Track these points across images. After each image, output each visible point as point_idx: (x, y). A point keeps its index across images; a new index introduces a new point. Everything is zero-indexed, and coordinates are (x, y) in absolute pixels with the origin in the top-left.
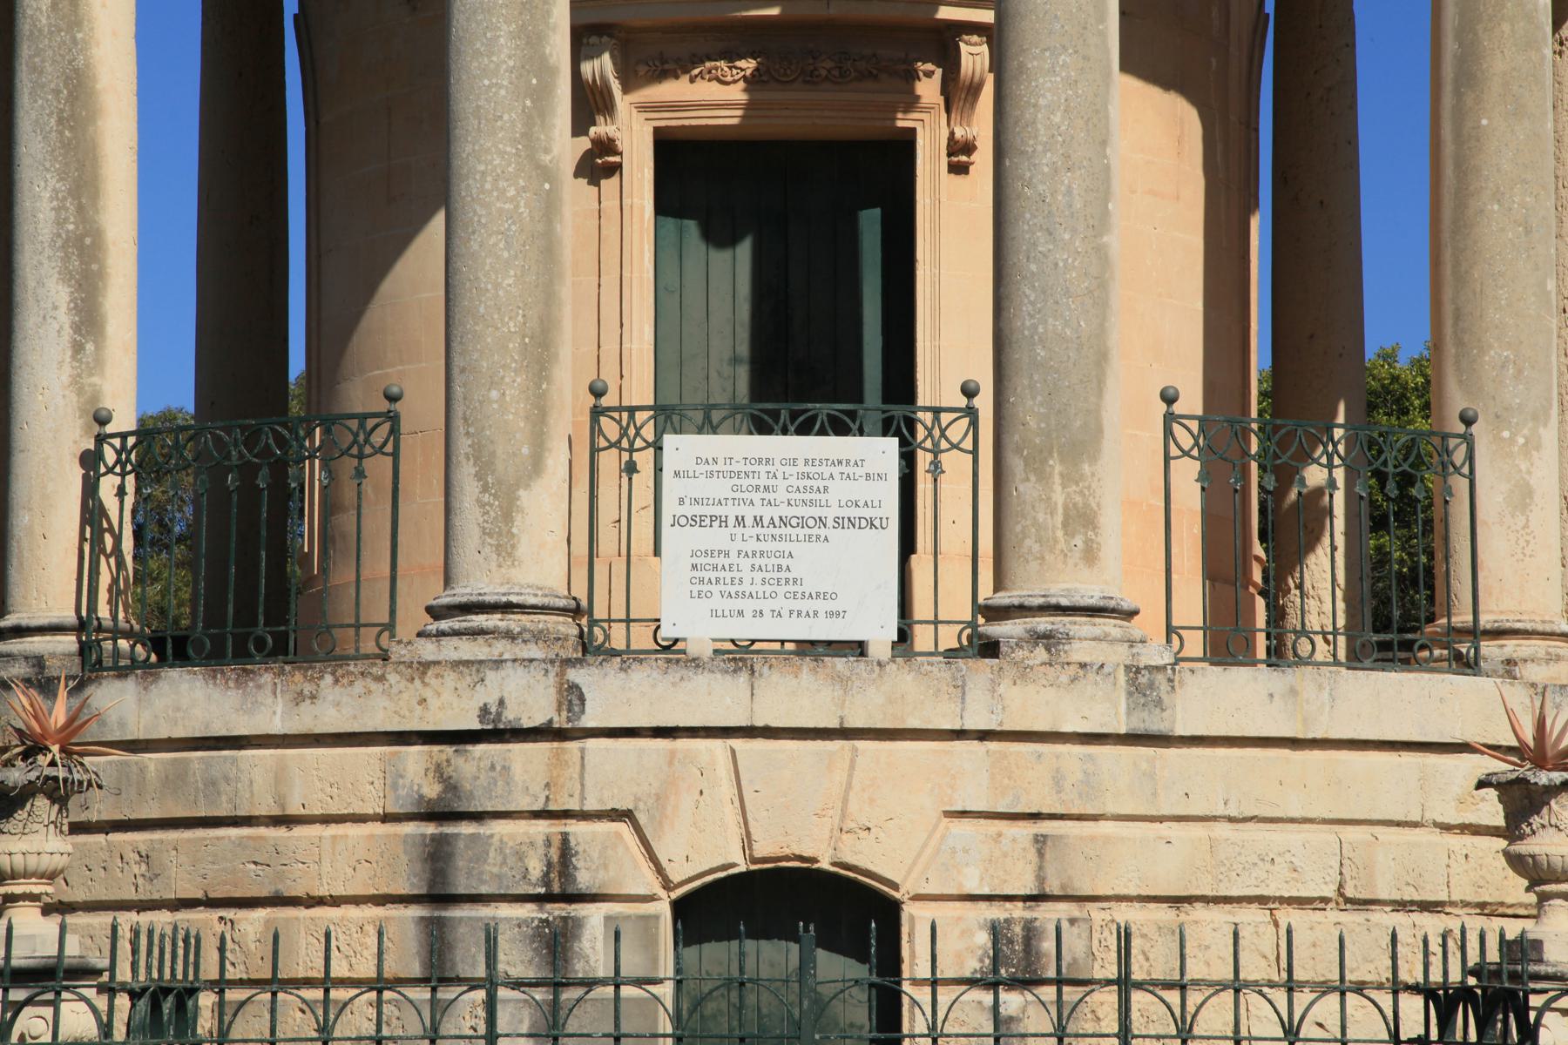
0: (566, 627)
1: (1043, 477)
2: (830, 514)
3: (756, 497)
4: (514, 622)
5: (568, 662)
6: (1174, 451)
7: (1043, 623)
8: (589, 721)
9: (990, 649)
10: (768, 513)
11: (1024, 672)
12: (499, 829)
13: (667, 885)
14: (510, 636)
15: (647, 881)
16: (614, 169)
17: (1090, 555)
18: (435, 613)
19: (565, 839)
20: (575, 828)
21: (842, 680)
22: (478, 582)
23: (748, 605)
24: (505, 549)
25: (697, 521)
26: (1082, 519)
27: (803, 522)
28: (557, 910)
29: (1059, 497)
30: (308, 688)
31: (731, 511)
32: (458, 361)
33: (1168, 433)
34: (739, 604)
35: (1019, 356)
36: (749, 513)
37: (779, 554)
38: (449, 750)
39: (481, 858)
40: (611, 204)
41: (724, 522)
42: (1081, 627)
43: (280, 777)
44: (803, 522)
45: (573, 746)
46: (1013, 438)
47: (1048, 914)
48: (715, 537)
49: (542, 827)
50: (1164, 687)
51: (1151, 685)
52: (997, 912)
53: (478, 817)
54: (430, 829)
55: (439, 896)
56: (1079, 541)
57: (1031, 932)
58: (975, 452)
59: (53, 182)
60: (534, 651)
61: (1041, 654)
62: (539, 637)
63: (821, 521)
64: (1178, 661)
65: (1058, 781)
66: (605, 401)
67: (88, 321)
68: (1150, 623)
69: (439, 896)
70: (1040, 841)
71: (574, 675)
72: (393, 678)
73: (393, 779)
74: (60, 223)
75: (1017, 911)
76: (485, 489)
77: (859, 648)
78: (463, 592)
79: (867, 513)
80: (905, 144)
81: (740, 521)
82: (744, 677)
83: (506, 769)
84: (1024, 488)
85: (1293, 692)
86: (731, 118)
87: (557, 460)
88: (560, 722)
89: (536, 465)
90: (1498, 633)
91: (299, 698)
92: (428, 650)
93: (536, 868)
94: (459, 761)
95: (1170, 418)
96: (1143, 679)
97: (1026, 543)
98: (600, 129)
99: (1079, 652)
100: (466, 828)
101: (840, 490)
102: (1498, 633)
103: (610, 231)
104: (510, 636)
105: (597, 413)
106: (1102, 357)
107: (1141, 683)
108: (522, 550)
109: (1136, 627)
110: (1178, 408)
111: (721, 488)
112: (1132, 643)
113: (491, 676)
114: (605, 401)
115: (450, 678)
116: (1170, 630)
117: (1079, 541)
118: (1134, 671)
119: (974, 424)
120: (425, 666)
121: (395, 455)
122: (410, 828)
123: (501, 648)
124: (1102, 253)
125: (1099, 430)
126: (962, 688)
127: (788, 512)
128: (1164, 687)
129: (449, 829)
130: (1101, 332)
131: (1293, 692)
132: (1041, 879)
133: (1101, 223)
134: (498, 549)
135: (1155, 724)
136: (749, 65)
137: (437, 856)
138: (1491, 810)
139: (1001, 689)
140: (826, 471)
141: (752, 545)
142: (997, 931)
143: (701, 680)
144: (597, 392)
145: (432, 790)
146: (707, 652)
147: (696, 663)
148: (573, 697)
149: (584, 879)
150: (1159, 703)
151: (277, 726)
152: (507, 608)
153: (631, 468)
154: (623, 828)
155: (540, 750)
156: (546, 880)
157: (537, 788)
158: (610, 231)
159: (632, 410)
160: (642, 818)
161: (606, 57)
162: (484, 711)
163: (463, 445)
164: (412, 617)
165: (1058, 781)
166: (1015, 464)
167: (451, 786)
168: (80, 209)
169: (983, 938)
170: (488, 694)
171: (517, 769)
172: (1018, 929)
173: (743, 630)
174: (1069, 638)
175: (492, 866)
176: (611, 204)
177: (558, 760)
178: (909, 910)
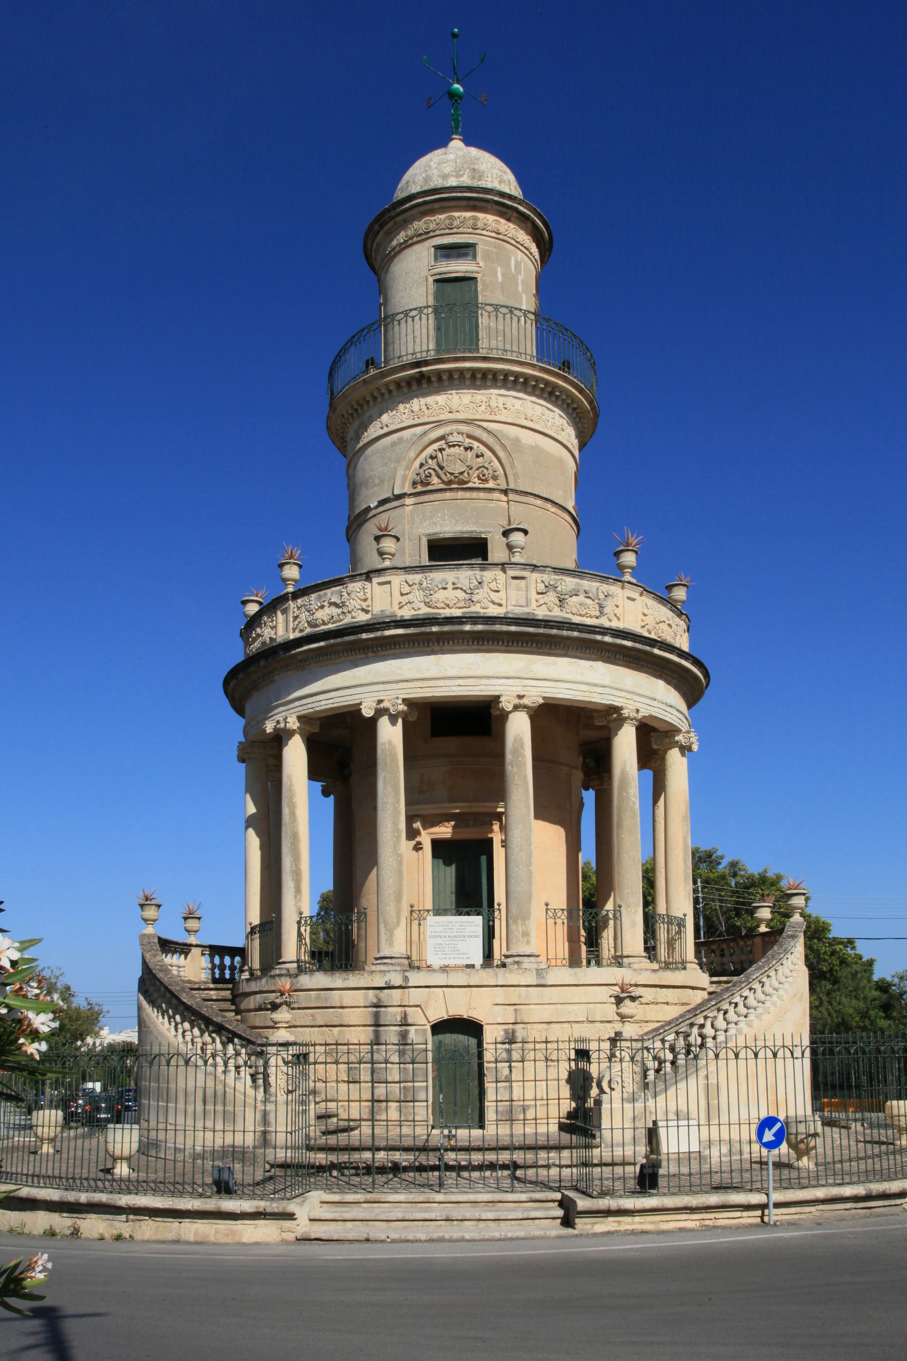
0: (406, 962)
1: (517, 924)
2: (466, 934)
3: (449, 931)
4: (393, 961)
5: (405, 971)
6: (548, 917)
7: (517, 959)
8: (410, 985)
9: (504, 965)
10: (452, 934)
11: (511, 971)
12: (390, 1009)
13: (429, 1022)
14: (392, 964)
15: (424, 1021)
16: (421, 849)
17: (528, 942)
18: (377, 959)
19: (405, 1012)
20: (407, 1009)
21: (469, 974)
22: (385, 952)
23: (447, 956)
24: (391, 942)
25: (435, 937)
26: (526, 934)
27: (449, 936)
28: (404, 1028)
29: (520, 929)
30: (347, 977)
31: (443, 934)
32: (380, 900)
33: (547, 913)
34: (444, 956)
35: (511, 896)
36: (447, 935)
37: (455, 944)
38: (378, 991)
39: (387, 1016)
40: (421, 857)
41: (441, 937)
42: (525, 959)
43: (341, 997)
44: (460, 936)
45: (406, 990)
46: (510, 915)
47: (517, 1027)
48: (440, 941)
49: (400, 1009)
50: (545, 973)
51: (542, 973)
52: (506, 1027)
53: (386, 1007)
54: (375, 1009)
55: (377, 1025)
56: (525, 939)
57: (514, 1031)
58: (500, 919)
59: (290, 858)
60: (398, 968)
61: (516, 966)
62: (399, 964)
63: (464, 936)
64: (549, 967)
65: (520, 996)
66: (414, 909)
67: (298, 890)
68: (543, 958)
69: (377, 1025)
70: (516, 1010)
71: (406, 974)
72: (365, 975)
73: (366, 998)
74: (291, 867)
75: (511, 1026)
76: (386, 930)
77: (473, 966)
78: (382, 954)
79: (475, 934)
80: (491, 840)
81: (445, 937)
82: (445, 974)
83: (391, 996)
84: (513, 927)
85: (576, 973)
86: (449, 836)
87: (403, 923)
88: (403, 985)
89: (398, 924)
90: (627, 957)
91: (345, 979)
92: (373, 968)
93: (399, 1018)
94: (381, 994)
95: (547, 909)
96: (540, 972)
97: (513, 941)
98: (418, 839)
99: (525, 966)
100: (383, 1009)
101: (468, 929)
102: (627, 957)
103: (421, 863)
104: (392, 964)
105: (412, 911)
106: (531, 896)
107: (539, 973)
108: (395, 944)
109: (539, 959)
110: (549, 907)
111: (440, 929)
112: (538, 963)
113: (387, 974)
114: (414, 909)
115: (378, 974)
116: (548, 959)
117: (525, 939)
118: (537, 970)
119: (500, 912)
120: (373, 972)
121: (366, 922)
122: (370, 1009)
123: (390, 968)
124: (530, 872)
125: (530, 913)
126: (497, 975)
127: (456, 934)
128: (545, 973)
129: (379, 1009)
130: (530, 890)
131: (576, 973)
132: (516, 1019)
133: (529, 864)
134: (390, 944)
135: (543, 982)
136: (453, 823)
137: (377, 1016)
138: (613, 1000)
139: (506, 975)
140: (465, 924)
141: (448, 943)
142: (506, 1031)
143: (435, 975)
144: (412, 907)
145: (375, 1001)
146: (438, 967)
147: (434, 971)
148: (406, 979)
149: (410, 1021)
150: (543, 977)
151: (340, 986)
152: (391, 958)
153: (420, 924)
154: (419, 1009)
155: (400, 991)
156: (401, 1021)
157: (398, 999)
158: (421, 863)
159: (420, 911)
160: (423, 1007)
161: (419, 823)
162: (386, 982)
163: (381, 920)
164: (370, 959)
165: (520, 996)
166: (511, 921)
167: (379, 1000)
168: (296, 865)
169: (502, 1033)
170: (387, 978)
171: (394, 995)
172: (510, 1031)
173: (446, 962)
174: (523, 962)
175: (389, 1018)
176: (421, 857)
177: (403, 993)
178: (485, 1027)
